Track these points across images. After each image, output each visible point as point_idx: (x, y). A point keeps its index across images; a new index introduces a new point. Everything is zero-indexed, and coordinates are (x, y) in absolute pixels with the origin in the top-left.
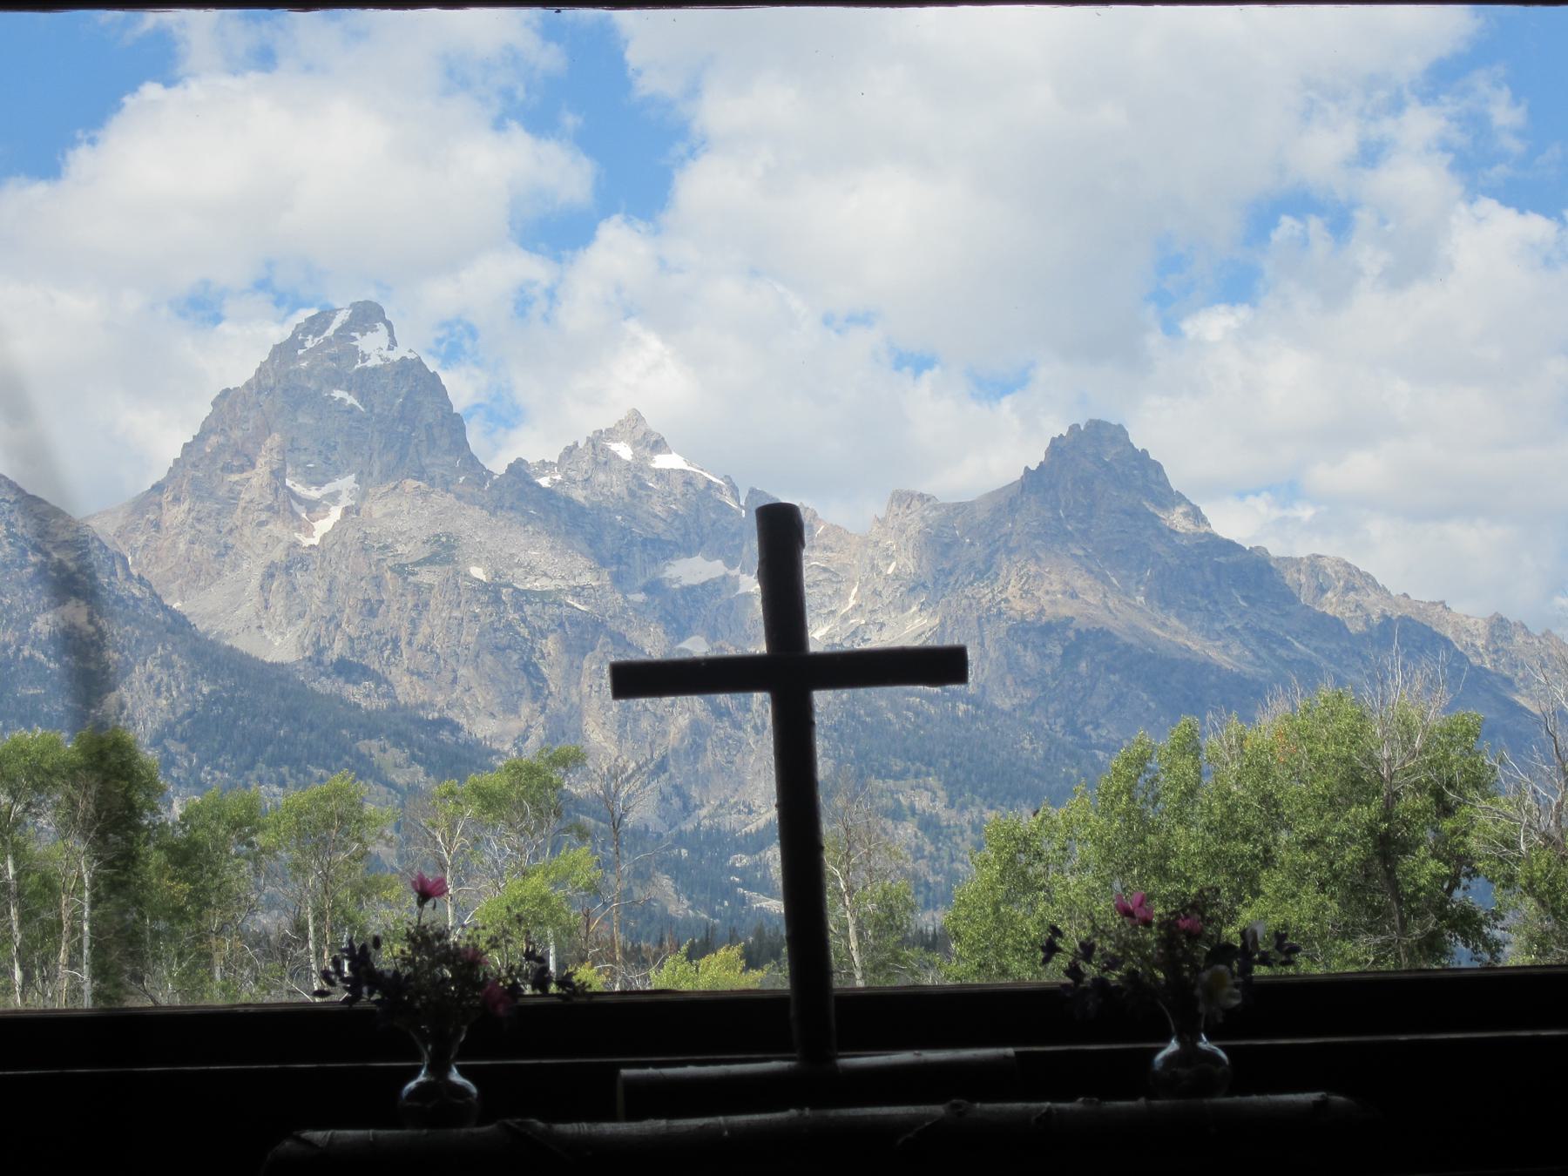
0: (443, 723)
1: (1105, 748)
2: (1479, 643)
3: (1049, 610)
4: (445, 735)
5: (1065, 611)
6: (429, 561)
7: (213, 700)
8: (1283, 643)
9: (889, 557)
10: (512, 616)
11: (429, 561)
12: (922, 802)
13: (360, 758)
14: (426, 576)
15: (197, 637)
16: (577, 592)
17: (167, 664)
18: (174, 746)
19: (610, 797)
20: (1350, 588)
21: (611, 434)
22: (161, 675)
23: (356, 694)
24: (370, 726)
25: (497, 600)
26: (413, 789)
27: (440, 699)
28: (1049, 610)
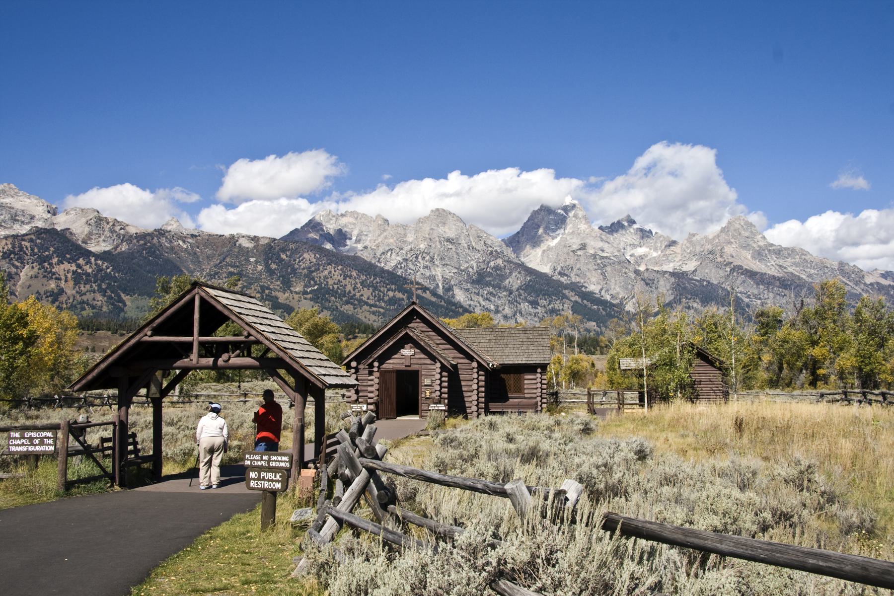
0: (583, 286)
1: (740, 293)
2: (836, 268)
3: (727, 260)
4: (583, 289)
5: (730, 261)
6: (580, 249)
7: (530, 281)
8: (785, 268)
9: (688, 248)
10: (599, 262)
11: (580, 249)
12: (695, 305)
13: (563, 294)
14: (579, 253)
15: (526, 267)
16: (614, 256)
17: (520, 273)
18: (521, 291)
19: (621, 303)
20: (803, 254)
21: (623, 220)
22: (519, 276)
23: (563, 280)
24: (566, 287)
25: (595, 258)
26: (576, 302)
27: (582, 281)
28: (727, 260)
